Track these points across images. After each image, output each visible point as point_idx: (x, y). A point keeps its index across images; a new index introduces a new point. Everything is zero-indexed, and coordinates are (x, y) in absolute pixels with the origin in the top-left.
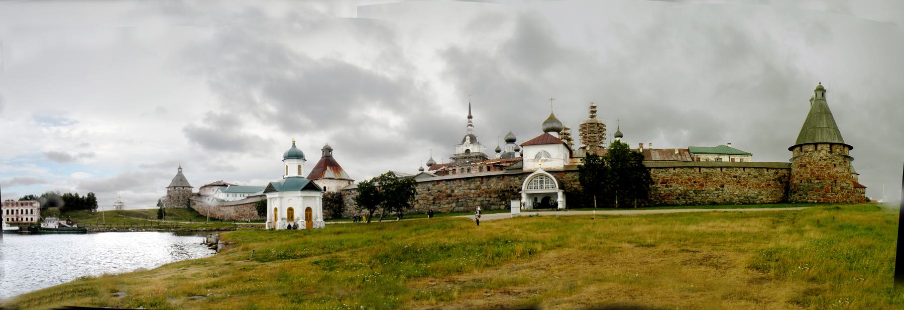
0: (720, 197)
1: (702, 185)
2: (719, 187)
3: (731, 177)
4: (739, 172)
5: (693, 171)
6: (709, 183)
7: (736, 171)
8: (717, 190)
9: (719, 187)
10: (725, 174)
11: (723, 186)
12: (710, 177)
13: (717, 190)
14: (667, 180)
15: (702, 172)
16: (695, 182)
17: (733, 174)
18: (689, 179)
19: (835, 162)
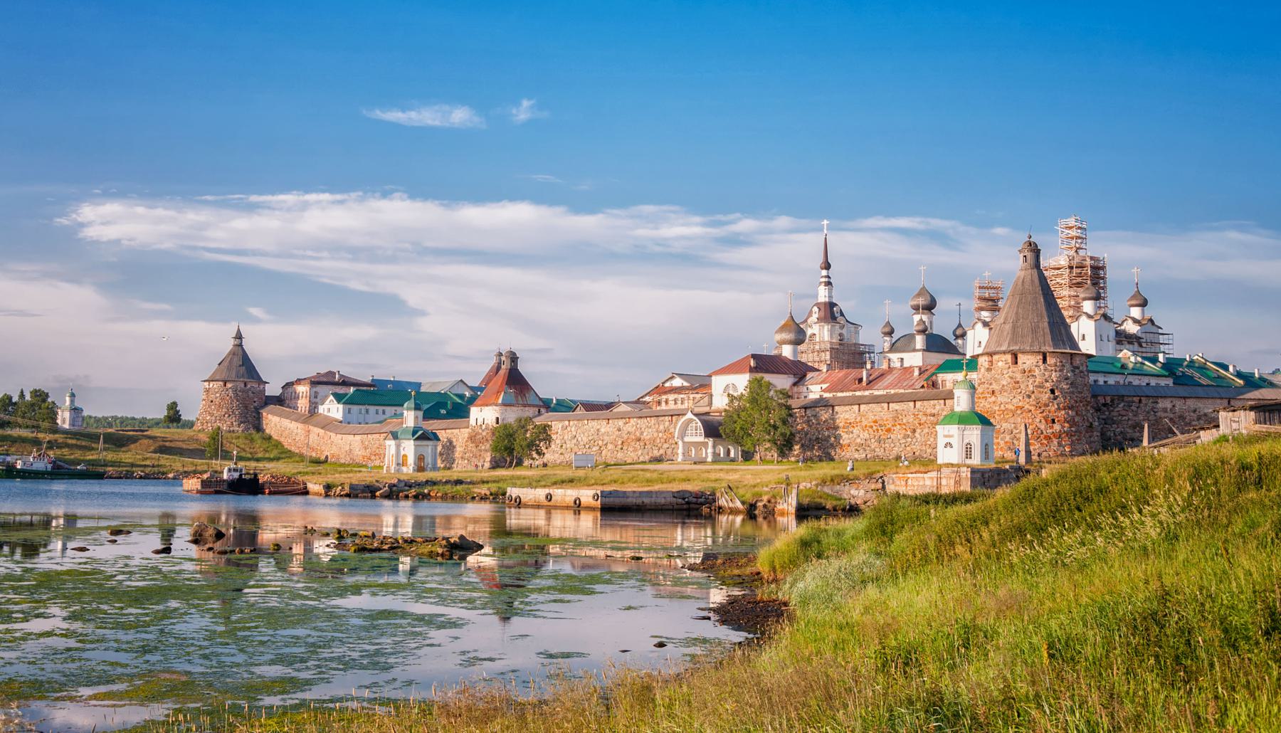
0: (908, 449)
1: (889, 430)
2: (909, 433)
3: (926, 415)
4: (938, 407)
5: (880, 409)
6: (898, 426)
7: (934, 405)
8: (906, 437)
9: (909, 433)
10: (919, 411)
11: (914, 431)
12: (900, 417)
13: (906, 437)
14: (850, 423)
15: (891, 409)
16: (881, 425)
17: (929, 411)
18: (875, 422)
19: (995, 387)
